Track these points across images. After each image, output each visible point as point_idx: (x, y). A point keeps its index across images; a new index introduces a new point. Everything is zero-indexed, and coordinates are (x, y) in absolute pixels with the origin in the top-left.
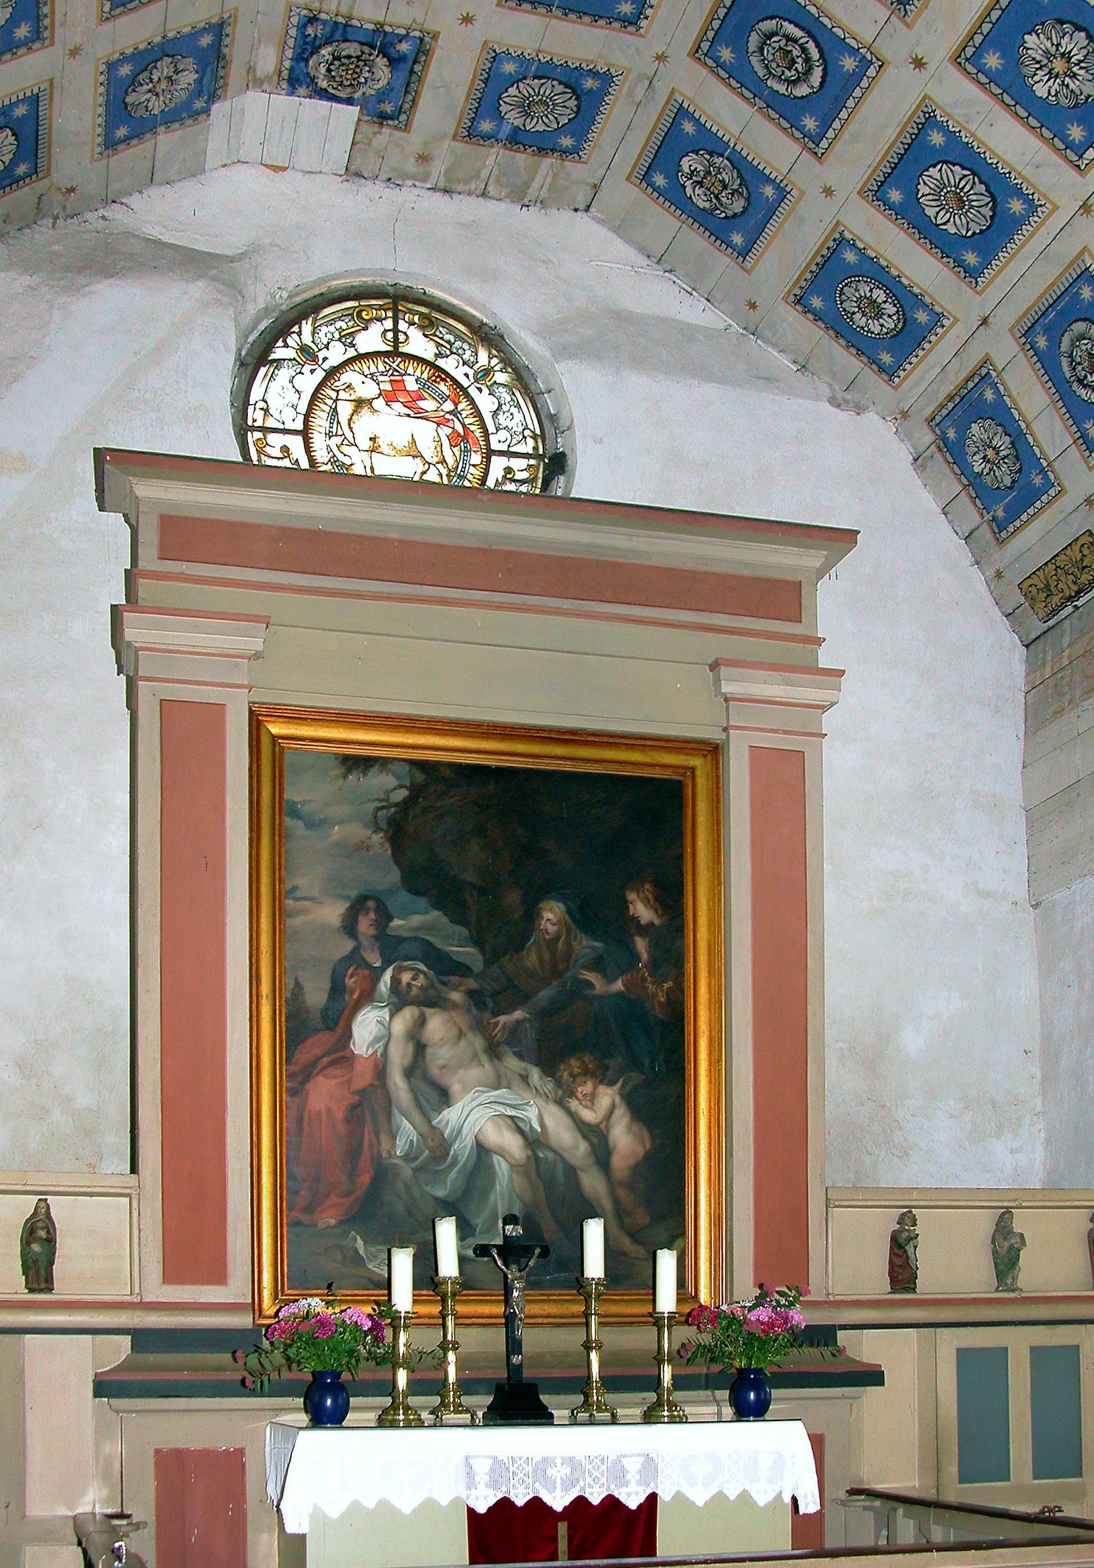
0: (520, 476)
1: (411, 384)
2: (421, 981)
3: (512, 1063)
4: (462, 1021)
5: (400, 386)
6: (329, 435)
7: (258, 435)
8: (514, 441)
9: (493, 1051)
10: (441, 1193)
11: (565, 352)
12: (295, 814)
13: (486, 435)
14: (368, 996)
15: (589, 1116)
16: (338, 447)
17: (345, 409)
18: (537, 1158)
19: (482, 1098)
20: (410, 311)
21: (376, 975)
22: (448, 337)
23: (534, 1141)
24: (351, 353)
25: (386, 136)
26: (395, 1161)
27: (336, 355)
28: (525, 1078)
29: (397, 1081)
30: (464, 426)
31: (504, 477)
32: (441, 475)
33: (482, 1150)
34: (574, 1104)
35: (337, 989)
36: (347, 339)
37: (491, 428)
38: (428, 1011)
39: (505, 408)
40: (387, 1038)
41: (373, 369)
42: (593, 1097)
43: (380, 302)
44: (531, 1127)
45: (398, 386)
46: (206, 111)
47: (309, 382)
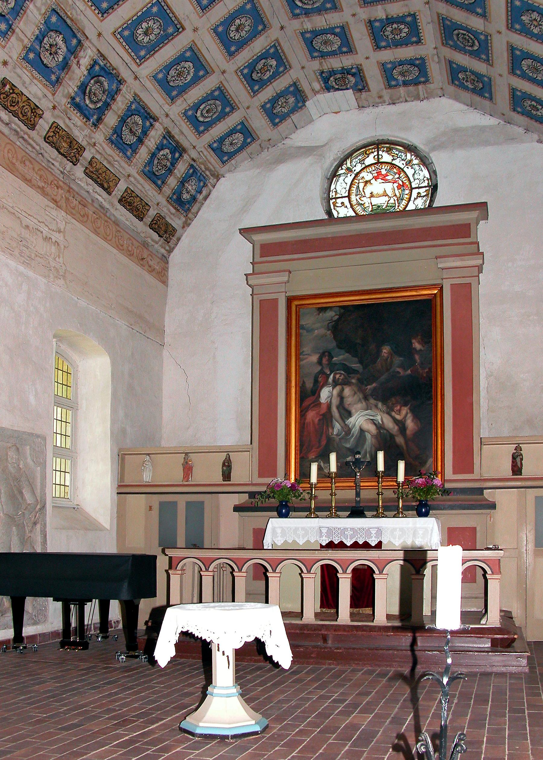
0: (423, 194)
1: (384, 172)
2: (342, 377)
3: (372, 401)
4: (355, 389)
5: (380, 173)
6: (357, 195)
7: (334, 200)
8: (421, 183)
9: (366, 398)
10: (348, 446)
11: (434, 149)
12: (303, 328)
13: (410, 183)
14: (325, 384)
15: (398, 417)
16: (360, 198)
17: (361, 185)
18: (380, 432)
19: (362, 414)
20: (383, 147)
21: (328, 376)
22: (396, 153)
23: (379, 427)
24: (363, 166)
25: (364, 95)
26: (333, 436)
27: (358, 168)
28: (376, 406)
29: (334, 410)
30: (402, 181)
31: (417, 196)
32: (395, 200)
33: (362, 431)
34: (393, 414)
35: (316, 381)
36: (362, 162)
37: (412, 180)
38: (345, 387)
39: (417, 172)
41: (371, 170)
42: (400, 411)
43: (373, 147)
44: (378, 422)
45: (379, 173)
46: (304, 105)
47: (349, 179)
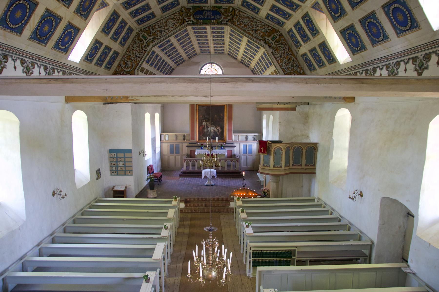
1: (213, 70)
3: (213, 125)
9: (212, 125)
14: (204, 121)
15: (218, 129)
23: (214, 130)
29: (205, 127)
33: (211, 131)
40: (205, 124)
